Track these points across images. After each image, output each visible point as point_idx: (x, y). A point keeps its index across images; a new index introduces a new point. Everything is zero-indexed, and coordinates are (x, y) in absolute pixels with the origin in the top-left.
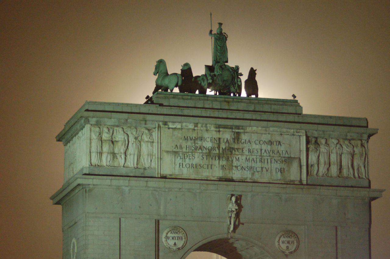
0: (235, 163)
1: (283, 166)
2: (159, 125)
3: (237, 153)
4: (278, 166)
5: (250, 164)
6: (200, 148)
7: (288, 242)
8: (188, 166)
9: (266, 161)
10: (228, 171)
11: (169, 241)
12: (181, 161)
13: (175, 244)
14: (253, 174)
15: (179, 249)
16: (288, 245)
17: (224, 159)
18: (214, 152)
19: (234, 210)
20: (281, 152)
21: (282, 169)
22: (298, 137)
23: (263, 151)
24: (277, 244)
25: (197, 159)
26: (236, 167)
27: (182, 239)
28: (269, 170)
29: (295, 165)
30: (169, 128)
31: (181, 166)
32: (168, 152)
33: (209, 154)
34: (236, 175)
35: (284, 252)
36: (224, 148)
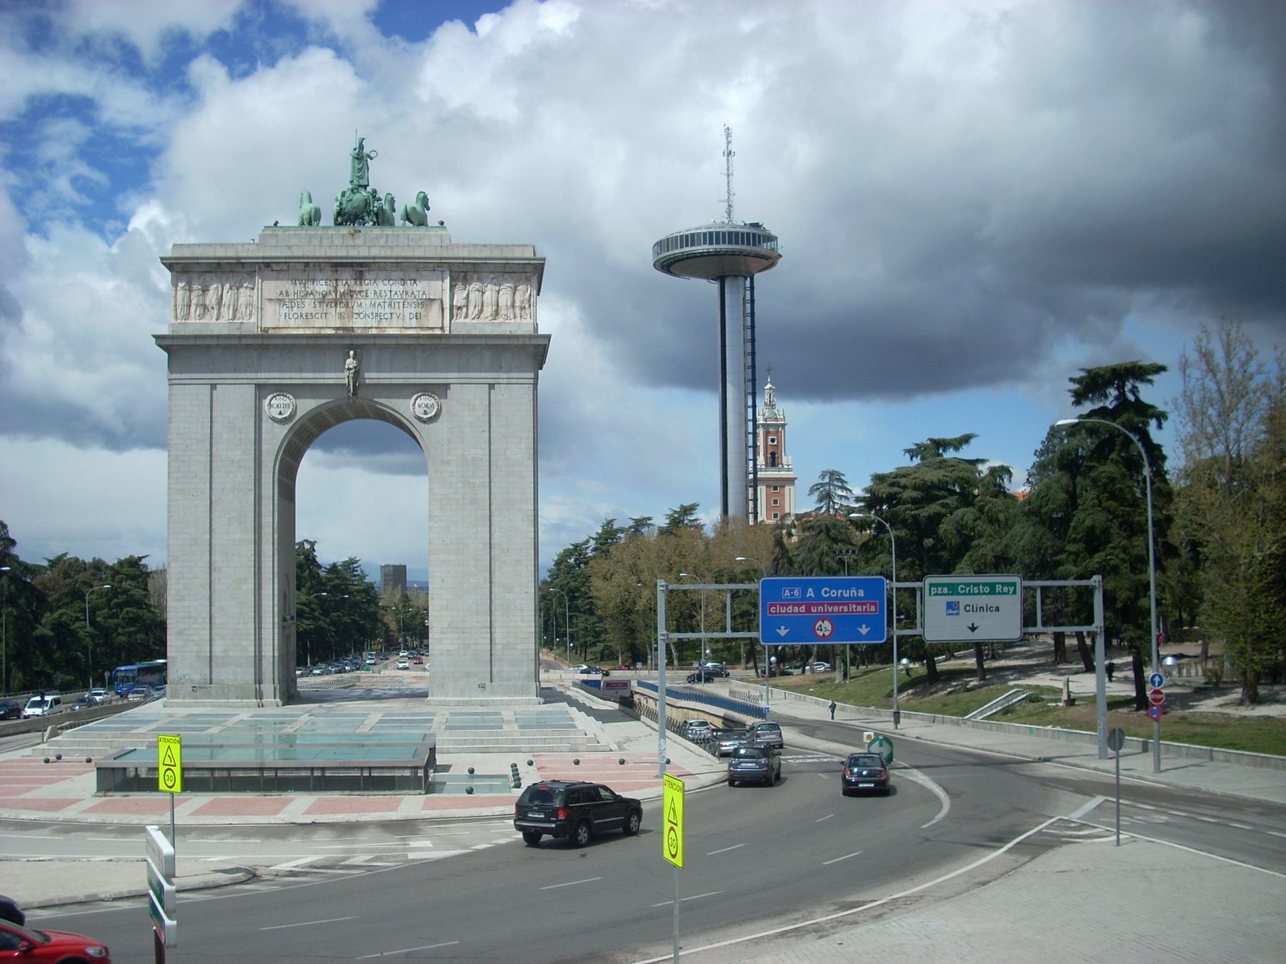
0: (356, 311)
1: (418, 310)
2: (260, 268)
3: (359, 296)
4: (413, 311)
5: (375, 311)
6: (312, 293)
7: (426, 406)
8: (296, 316)
9: (397, 305)
10: (347, 320)
11: (272, 410)
12: (287, 311)
13: (280, 413)
14: (379, 322)
15: (283, 421)
16: (426, 409)
17: (342, 305)
18: (330, 297)
19: (351, 366)
20: (416, 293)
21: (418, 315)
22: (440, 273)
23: (393, 293)
24: (411, 407)
25: (308, 306)
26: (358, 314)
27: (289, 407)
28: (401, 316)
29: (436, 306)
30: (273, 271)
31: (287, 318)
32: (270, 300)
33: (323, 300)
34: (358, 323)
35: (419, 419)
36: (342, 291)
